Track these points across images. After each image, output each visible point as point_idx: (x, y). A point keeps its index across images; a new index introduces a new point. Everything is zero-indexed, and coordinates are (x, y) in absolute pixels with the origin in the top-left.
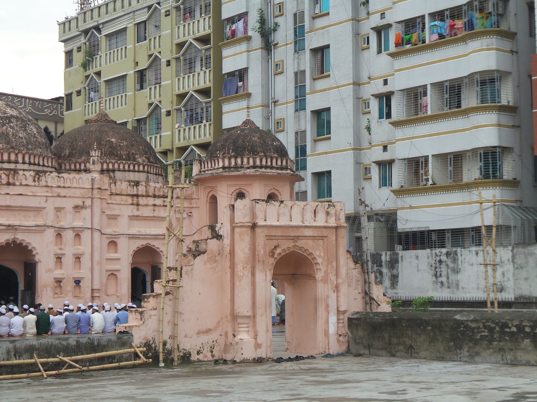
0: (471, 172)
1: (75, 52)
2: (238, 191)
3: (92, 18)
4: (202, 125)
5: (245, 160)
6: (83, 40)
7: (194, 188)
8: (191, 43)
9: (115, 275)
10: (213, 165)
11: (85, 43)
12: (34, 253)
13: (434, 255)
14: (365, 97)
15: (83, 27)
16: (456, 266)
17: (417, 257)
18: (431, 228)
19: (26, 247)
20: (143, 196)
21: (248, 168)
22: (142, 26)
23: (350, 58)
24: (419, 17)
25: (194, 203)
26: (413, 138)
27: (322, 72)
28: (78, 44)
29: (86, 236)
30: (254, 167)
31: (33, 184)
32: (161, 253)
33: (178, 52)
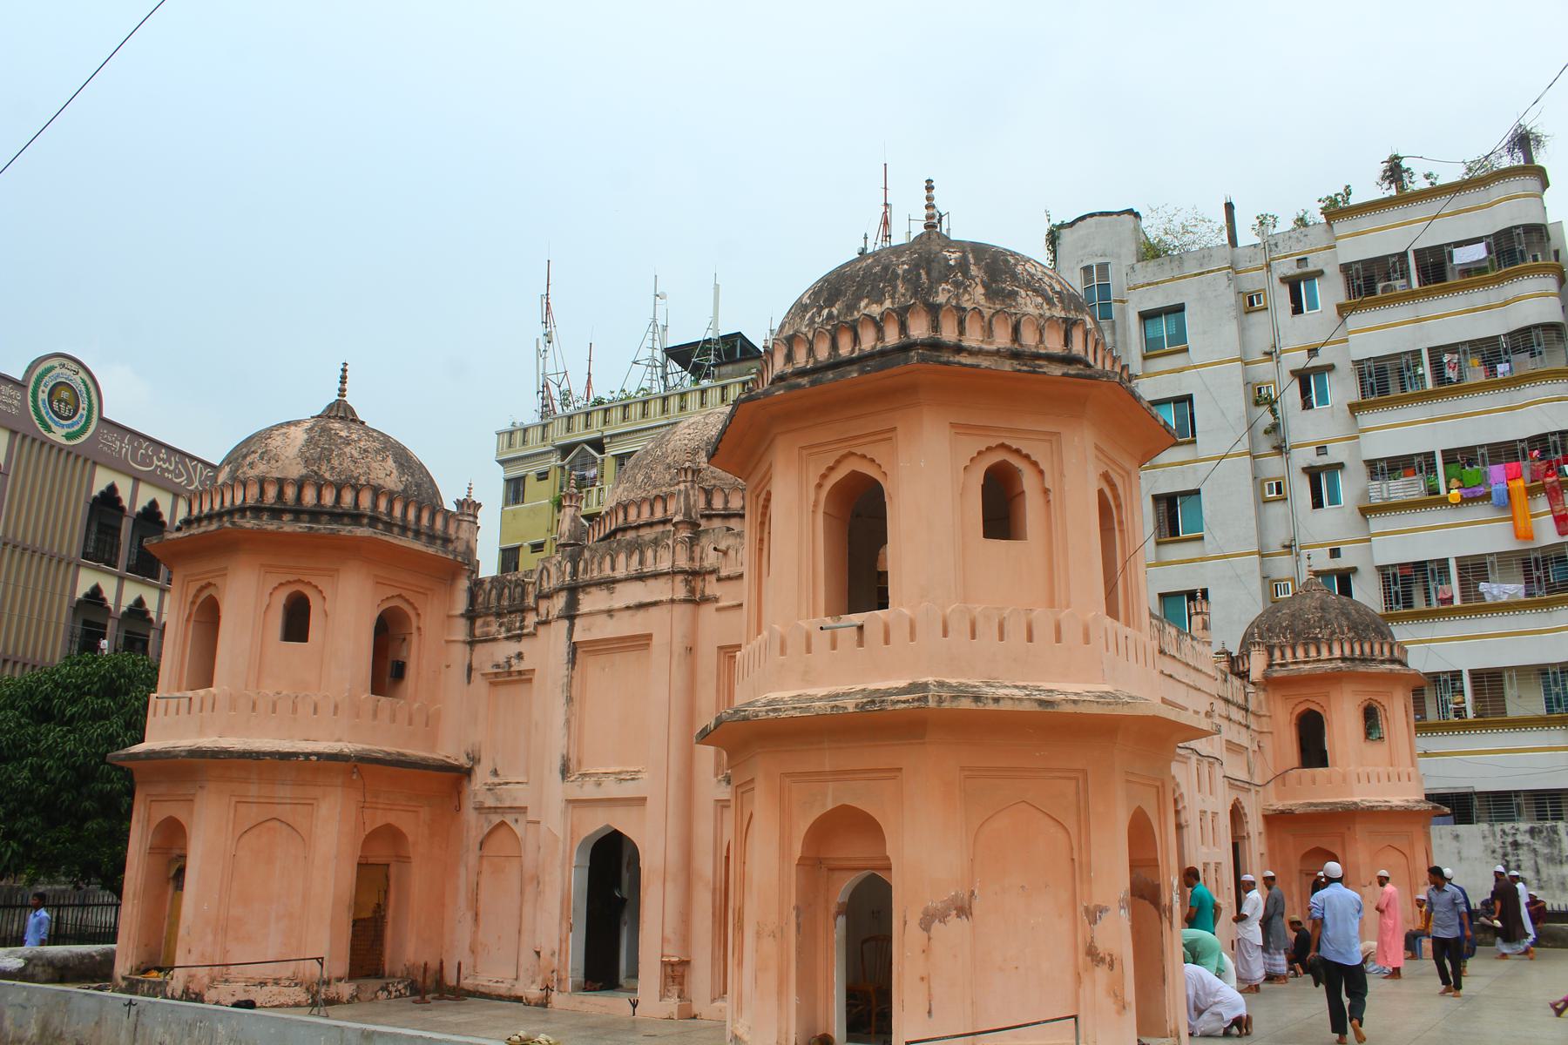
0: (1524, 701)
5: (1377, 647)
6: (555, 460)
7: (1262, 695)
10: (1313, 653)
11: (562, 467)
13: (1499, 834)
14: (1275, 576)
15: (559, 436)
16: (1556, 852)
17: (1457, 837)
18: (1478, 789)
21: (1382, 662)
23: (1252, 512)
24: (1418, 455)
25: (1265, 725)
26: (1431, 641)
27: (1174, 531)
28: (542, 468)
30: (1392, 661)
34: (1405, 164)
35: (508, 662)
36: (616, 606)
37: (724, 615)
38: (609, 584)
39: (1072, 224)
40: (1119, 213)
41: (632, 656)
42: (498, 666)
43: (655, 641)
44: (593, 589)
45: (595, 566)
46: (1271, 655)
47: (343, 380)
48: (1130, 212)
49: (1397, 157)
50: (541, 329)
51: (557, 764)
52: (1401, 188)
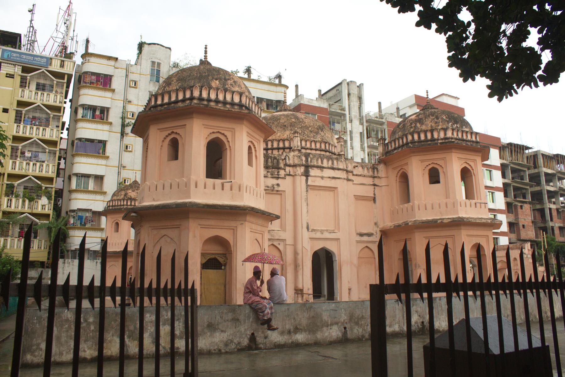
34: (252, 70)
35: (273, 186)
36: (325, 176)
37: (355, 186)
38: (321, 168)
39: (150, 44)
40: (166, 48)
41: (332, 193)
42: (268, 187)
43: (339, 190)
44: (315, 168)
45: (315, 161)
47: (206, 52)
48: (170, 49)
49: (250, 67)
51: (305, 226)
52: (249, 76)
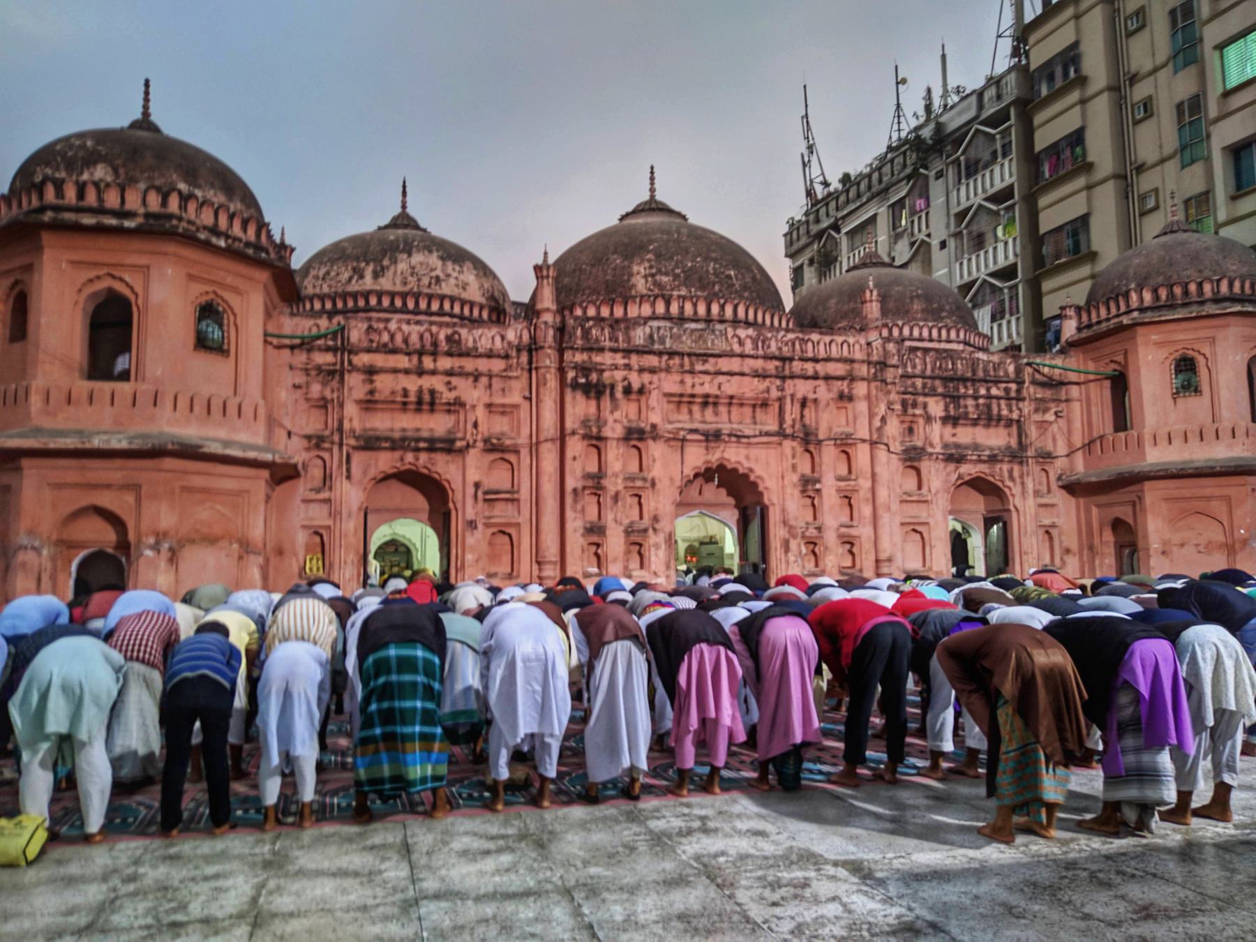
1: (805, 267)
2: (1177, 355)
3: (828, 215)
4: (1004, 322)
8: (980, 206)
9: (921, 533)
12: (761, 488)
15: (814, 229)
19: (746, 476)
20: (964, 380)
21: (1202, 303)
22: (897, 208)
29: (862, 454)
30: (1217, 300)
31: (752, 352)
32: (1006, 490)
33: (959, 223)
46: (1080, 318)
50: (804, 144)
